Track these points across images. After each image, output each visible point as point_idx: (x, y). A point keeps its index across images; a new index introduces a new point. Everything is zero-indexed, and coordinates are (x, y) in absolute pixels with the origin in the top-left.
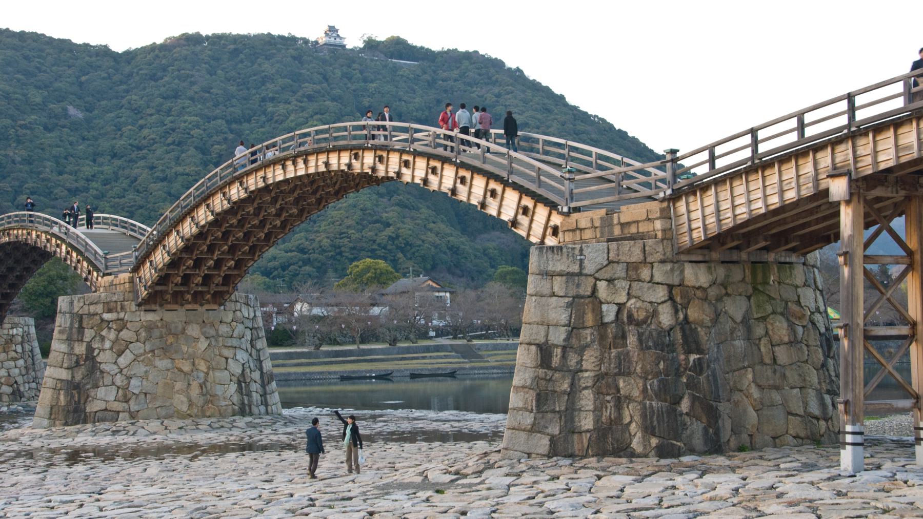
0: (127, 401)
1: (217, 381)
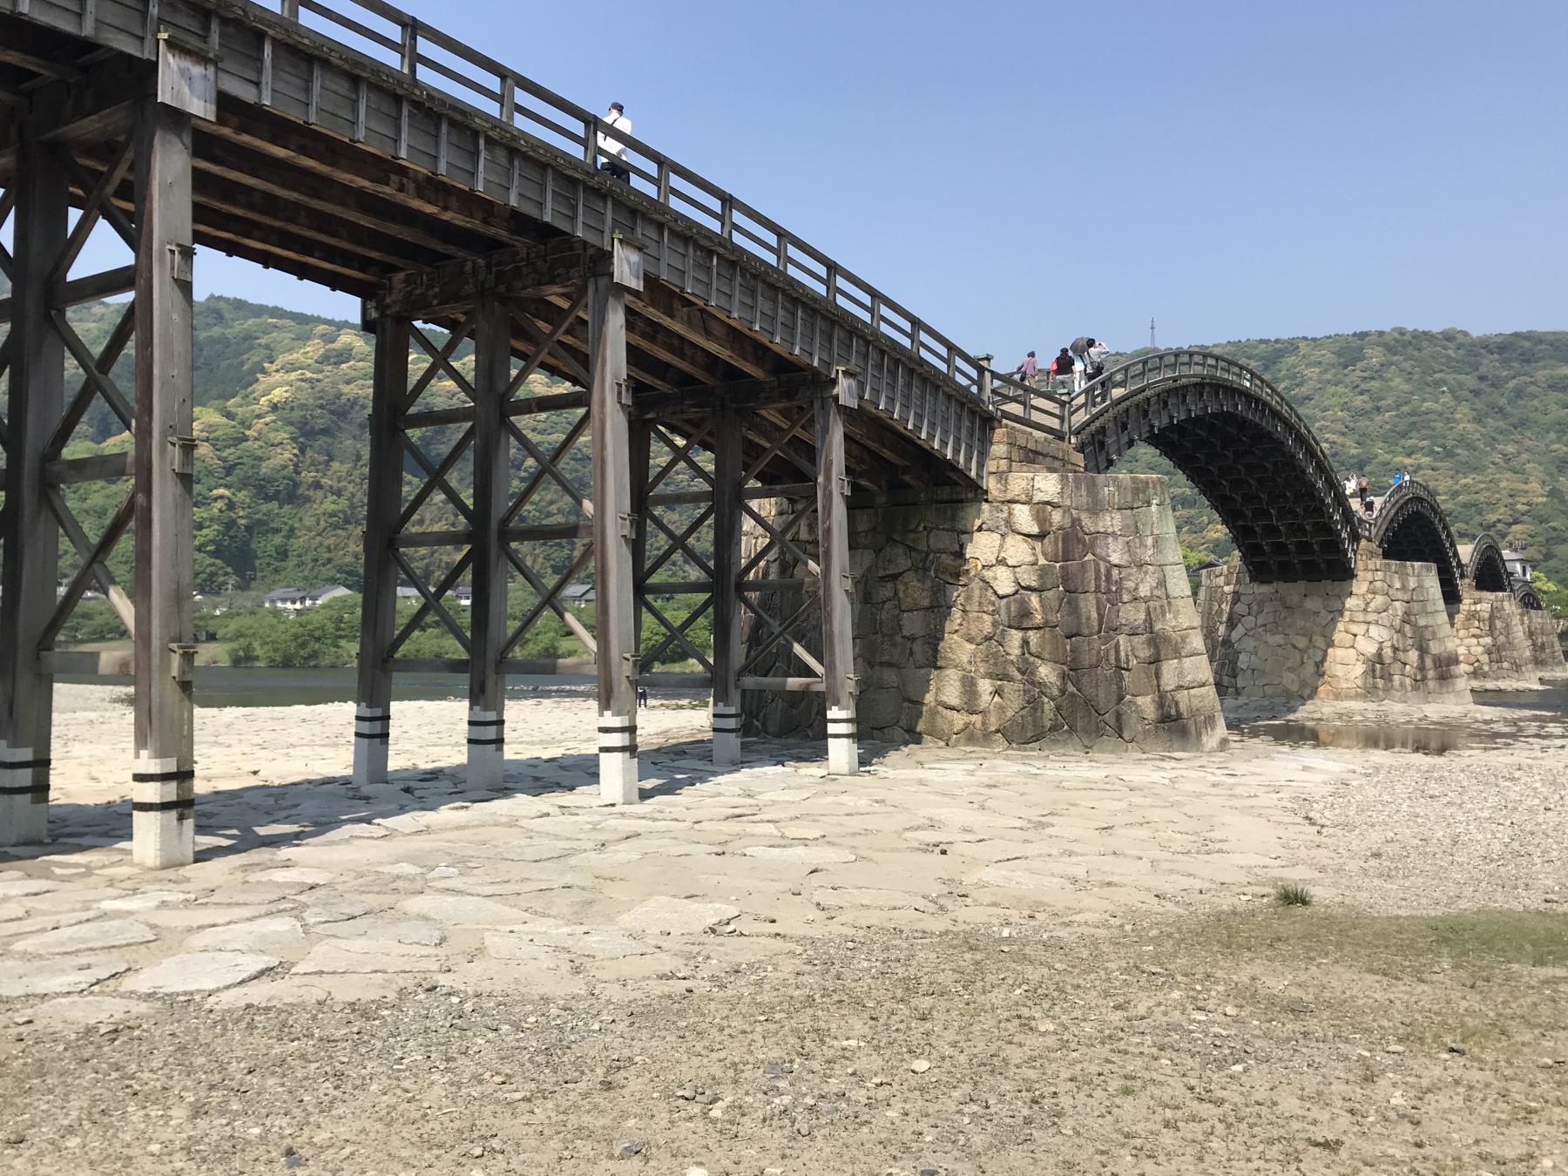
1: (1338, 660)
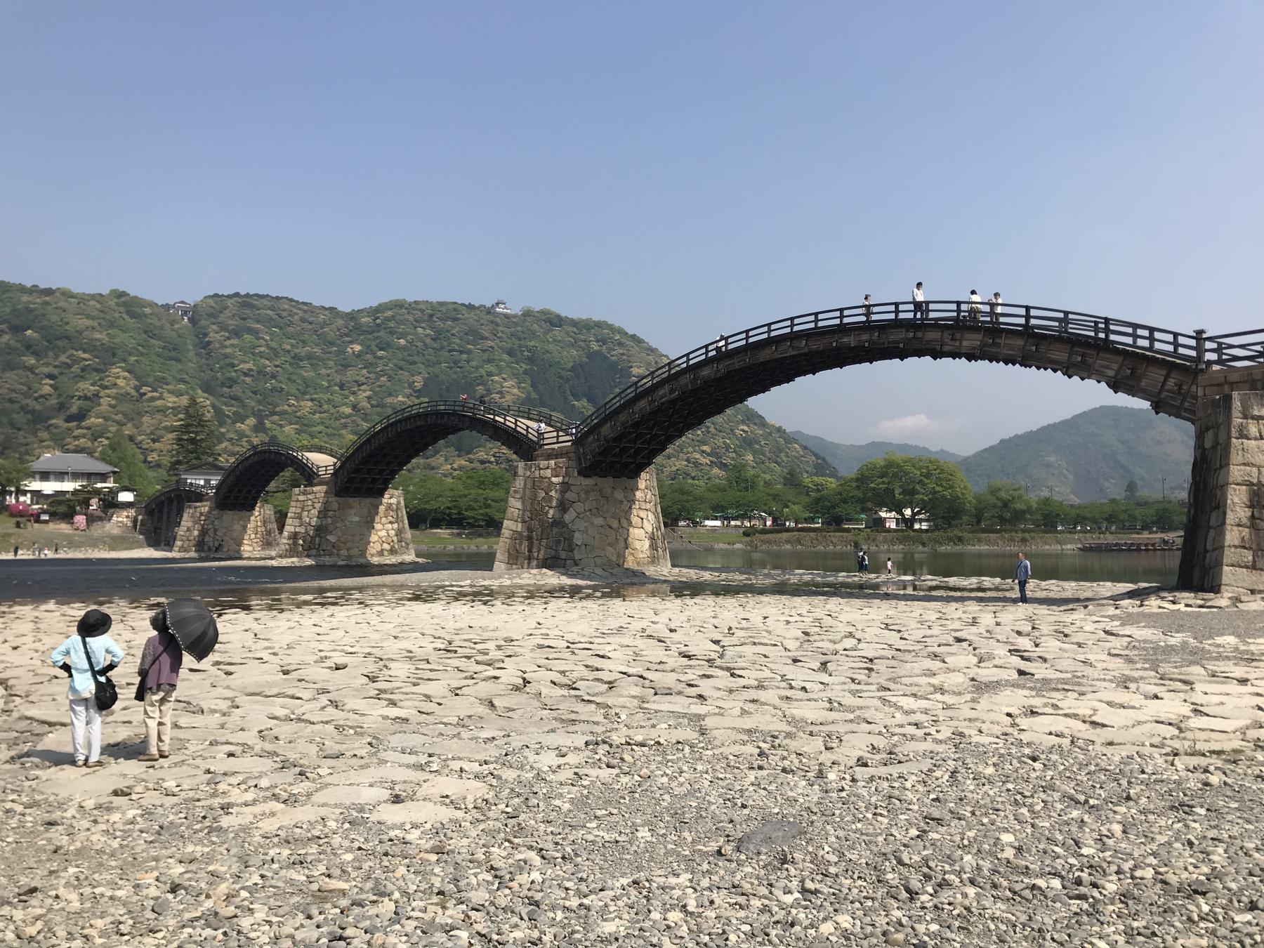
0: (572, 550)
